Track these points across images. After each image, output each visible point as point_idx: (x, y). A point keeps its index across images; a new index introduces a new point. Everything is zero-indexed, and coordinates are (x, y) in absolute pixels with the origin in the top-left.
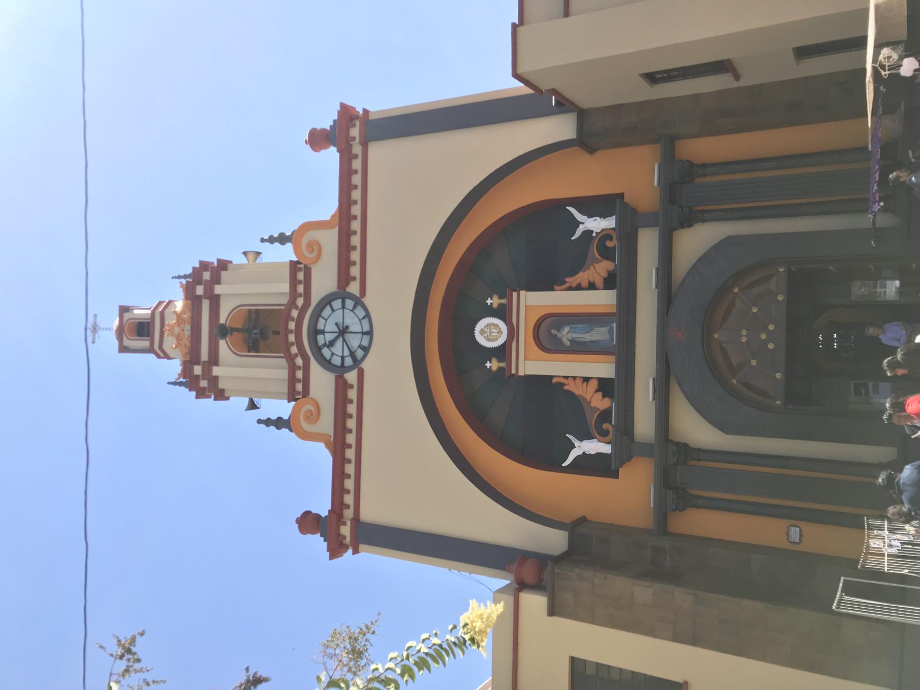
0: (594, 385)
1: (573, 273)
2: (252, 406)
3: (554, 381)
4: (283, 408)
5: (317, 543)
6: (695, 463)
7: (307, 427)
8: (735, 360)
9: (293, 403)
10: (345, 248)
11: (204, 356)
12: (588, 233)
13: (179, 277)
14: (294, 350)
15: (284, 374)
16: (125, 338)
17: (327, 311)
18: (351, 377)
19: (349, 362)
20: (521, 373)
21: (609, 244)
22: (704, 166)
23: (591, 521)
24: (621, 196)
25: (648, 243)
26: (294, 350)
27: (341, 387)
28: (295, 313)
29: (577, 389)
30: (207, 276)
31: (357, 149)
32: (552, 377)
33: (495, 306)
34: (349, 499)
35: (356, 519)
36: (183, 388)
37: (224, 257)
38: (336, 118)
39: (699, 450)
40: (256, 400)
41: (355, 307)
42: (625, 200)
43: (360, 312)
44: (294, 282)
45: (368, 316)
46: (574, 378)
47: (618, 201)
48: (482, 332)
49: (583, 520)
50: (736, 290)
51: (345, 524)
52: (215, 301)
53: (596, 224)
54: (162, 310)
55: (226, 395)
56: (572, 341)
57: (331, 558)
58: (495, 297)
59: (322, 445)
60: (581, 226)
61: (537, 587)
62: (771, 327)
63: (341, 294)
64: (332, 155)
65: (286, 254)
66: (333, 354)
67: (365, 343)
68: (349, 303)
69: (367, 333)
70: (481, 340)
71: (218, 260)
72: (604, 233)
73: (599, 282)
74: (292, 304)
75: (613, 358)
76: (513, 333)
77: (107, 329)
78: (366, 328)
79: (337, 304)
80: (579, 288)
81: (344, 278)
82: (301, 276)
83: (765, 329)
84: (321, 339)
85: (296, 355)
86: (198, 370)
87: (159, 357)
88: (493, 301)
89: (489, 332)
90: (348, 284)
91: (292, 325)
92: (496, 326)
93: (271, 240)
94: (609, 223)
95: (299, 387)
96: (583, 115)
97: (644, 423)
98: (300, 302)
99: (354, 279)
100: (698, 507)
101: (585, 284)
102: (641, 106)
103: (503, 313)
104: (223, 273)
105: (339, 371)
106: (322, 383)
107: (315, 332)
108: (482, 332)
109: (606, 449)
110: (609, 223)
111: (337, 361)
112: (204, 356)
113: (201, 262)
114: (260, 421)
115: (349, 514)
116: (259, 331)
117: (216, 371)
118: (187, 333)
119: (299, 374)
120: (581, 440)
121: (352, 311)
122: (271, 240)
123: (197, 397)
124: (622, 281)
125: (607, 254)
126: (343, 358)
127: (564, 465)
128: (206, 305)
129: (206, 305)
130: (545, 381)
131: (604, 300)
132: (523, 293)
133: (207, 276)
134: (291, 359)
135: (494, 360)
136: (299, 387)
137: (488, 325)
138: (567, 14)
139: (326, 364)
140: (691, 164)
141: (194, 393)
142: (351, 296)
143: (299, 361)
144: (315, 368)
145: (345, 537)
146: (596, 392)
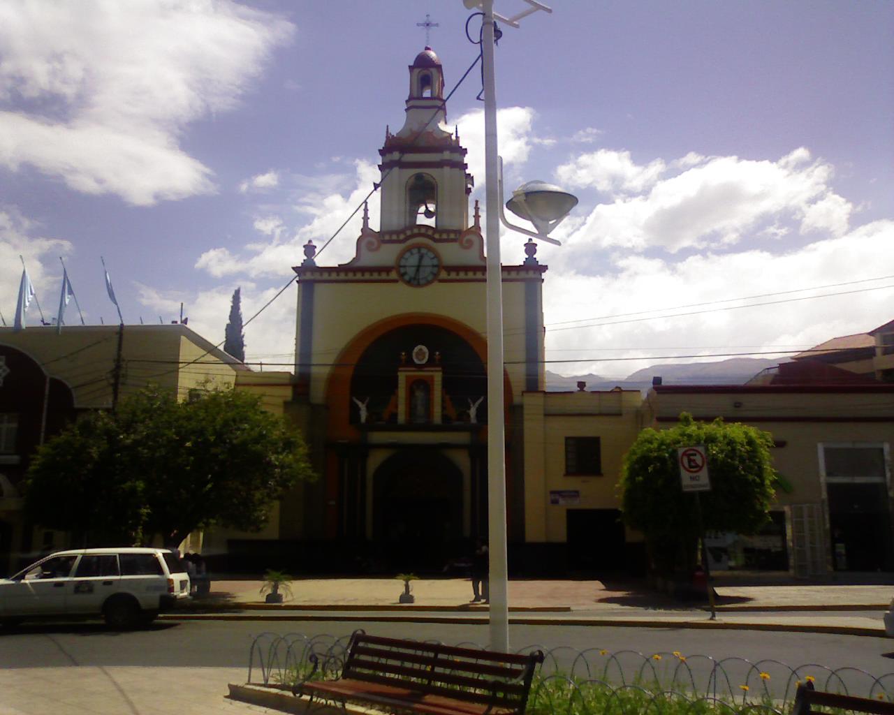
5: (299, 258)
7: (363, 244)
10: (466, 269)
12: (469, 408)
13: (456, 132)
14: (409, 233)
16: (420, 70)
18: (393, 275)
19: (402, 270)
20: (399, 374)
27: (387, 270)
28: (430, 233)
30: (456, 157)
31: (523, 275)
36: (385, 139)
38: (540, 264)
40: (380, 189)
44: (448, 232)
45: (429, 283)
48: (421, 349)
51: (312, 274)
52: (439, 165)
53: (473, 412)
57: (293, 268)
59: (354, 254)
61: (295, 394)
63: (441, 267)
66: (407, 259)
68: (435, 270)
69: (419, 282)
70: (416, 349)
71: (466, 164)
77: (428, 37)
78: (422, 282)
80: (443, 401)
81: (450, 269)
82: (452, 236)
84: (415, 251)
85: (405, 234)
87: (407, 101)
89: (421, 353)
90: (446, 270)
92: (424, 357)
94: (473, 420)
95: (387, 237)
97: (378, 437)
99: (449, 275)
103: (431, 362)
104: (456, 171)
105: (398, 267)
108: (421, 349)
110: (473, 420)
113: (466, 149)
115: (317, 276)
117: (396, 170)
119: (394, 237)
121: (432, 273)
123: (380, 150)
126: (404, 266)
130: (396, 387)
131: (437, 417)
132: (441, 373)
133: (456, 157)
134: (403, 231)
138: (547, 415)
139: (401, 256)
141: (382, 148)
143: (402, 237)
145: (305, 275)
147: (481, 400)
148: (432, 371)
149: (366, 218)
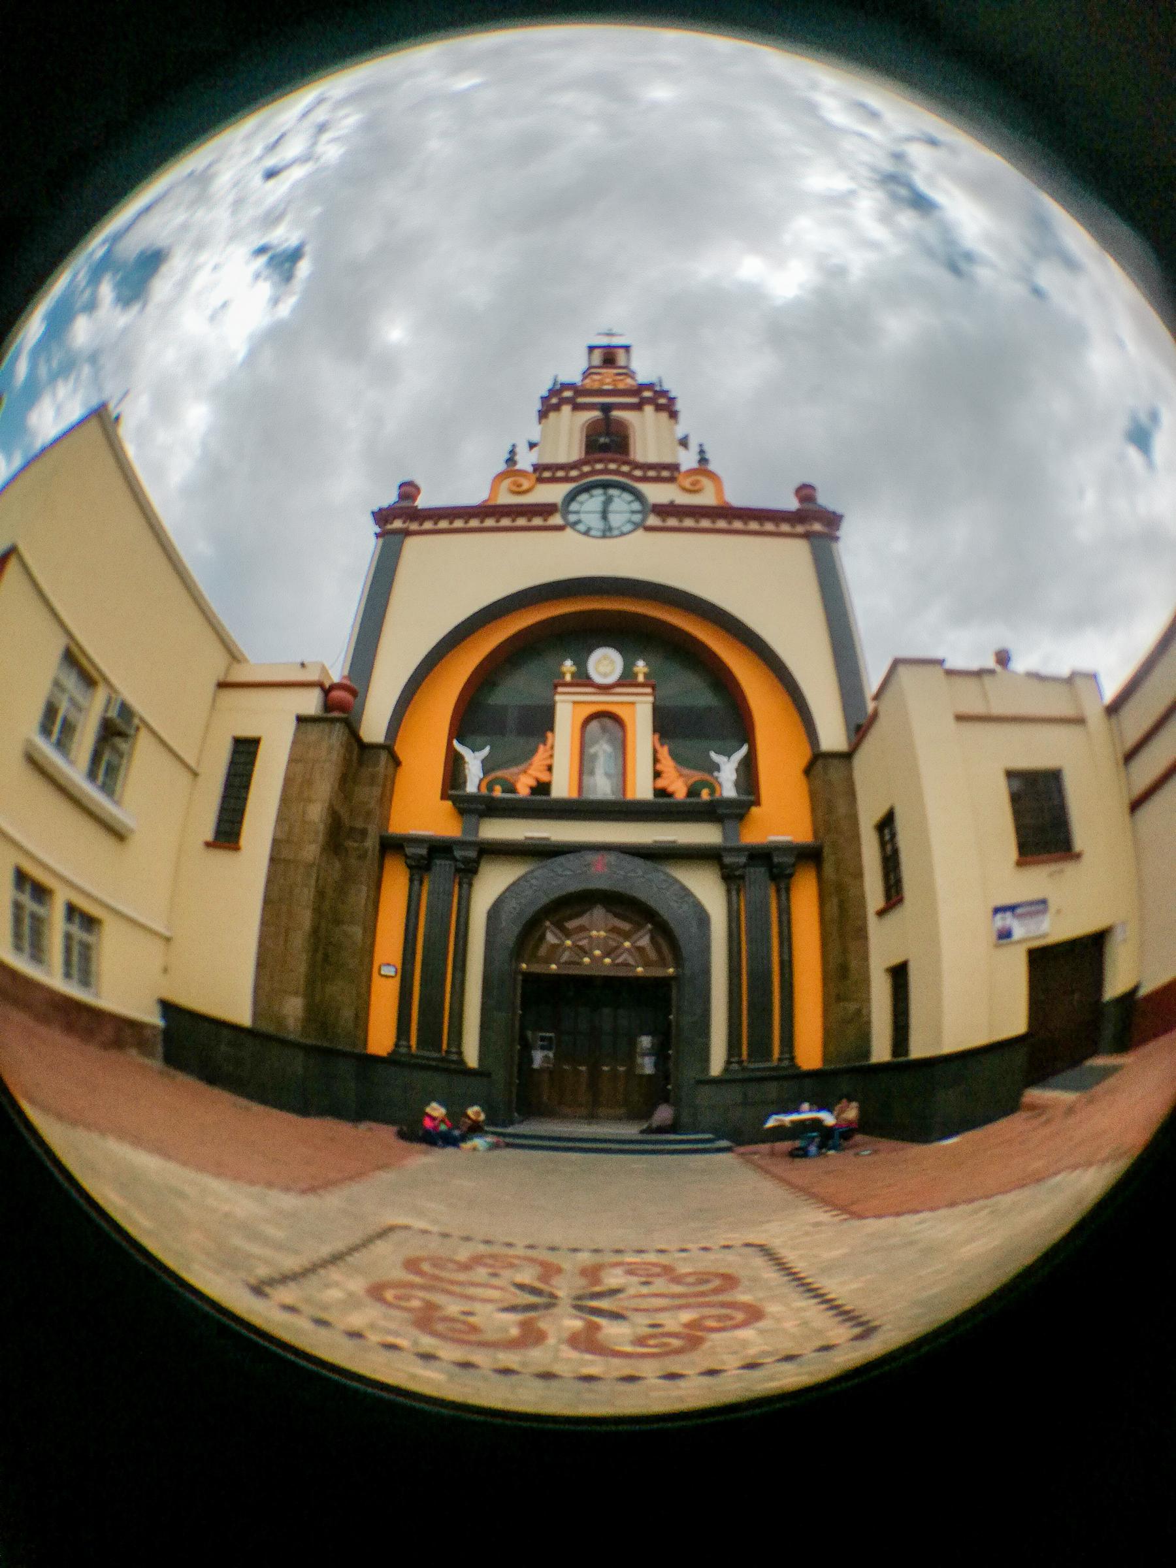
0: (544, 777)
1: (674, 755)
2: (532, 446)
3: (549, 734)
4: (526, 461)
6: (457, 880)
8: (571, 925)
9: (530, 469)
11: (581, 400)
12: (717, 768)
15: (562, 459)
17: (627, 497)
18: (556, 520)
19: (572, 518)
20: (558, 698)
21: (705, 795)
22: (788, 890)
23: (396, 771)
24: (757, 803)
25: (705, 834)
26: (586, 469)
27: (546, 510)
29: (539, 759)
30: (662, 401)
32: (552, 729)
33: (636, 669)
34: (428, 525)
35: (408, 533)
37: (682, 417)
39: (470, 885)
40: (535, 449)
41: (634, 523)
42: (754, 809)
43: (629, 527)
45: (623, 534)
46: (551, 756)
47: (752, 798)
49: (397, 763)
50: (649, 926)
54: (631, 374)
55: (543, 421)
56: (594, 757)
58: (646, 670)
60: (725, 759)
62: (607, 960)
64: (793, 504)
65: (687, 460)
66: (582, 503)
67: (593, 533)
68: (637, 518)
72: (717, 787)
73: (661, 783)
74: (637, 466)
75: (574, 795)
76: (605, 689)
79: (636, 506)
80: (656, 760)
81: (665, 510)
83: (607, 954)
84: (598, 492)
86: (568, 394)
88: (641, 666)
89: (605, 663)
91: (612, 466)
93: (702, 452)
96: (847, 757)
98: (638, 473)
100: (411, 881)
101: (659, 767)
102: (853, 818)
103: (627, 679)
106: (553, 493)
107: (606, 485)
109: (471, 788)
111: (574, 506)
112: (581, 400)
114: (514, 446)
115: (414, 526)
116: (608, 441)
117: (566, 409)
118: (606, 387)
119: (560, 474)
120: (483, 762)
121: (630, 521)
122: (702, 452)
124: (662, 809)
125: (693, 792)
126: (577, 512)
127: (455, 743)
128: (634, 400)
129: (634, 400)
132: (650, 699)
135: (574, 669)
136: (547, 474)
137: (612, 662)
139: (572, 497)
140: (791, 876)
142: (644, 520)
144: (567, 488)
146: (538, 781)
147: (744, 750)
148: (628, 694)
149: (511, 460)
